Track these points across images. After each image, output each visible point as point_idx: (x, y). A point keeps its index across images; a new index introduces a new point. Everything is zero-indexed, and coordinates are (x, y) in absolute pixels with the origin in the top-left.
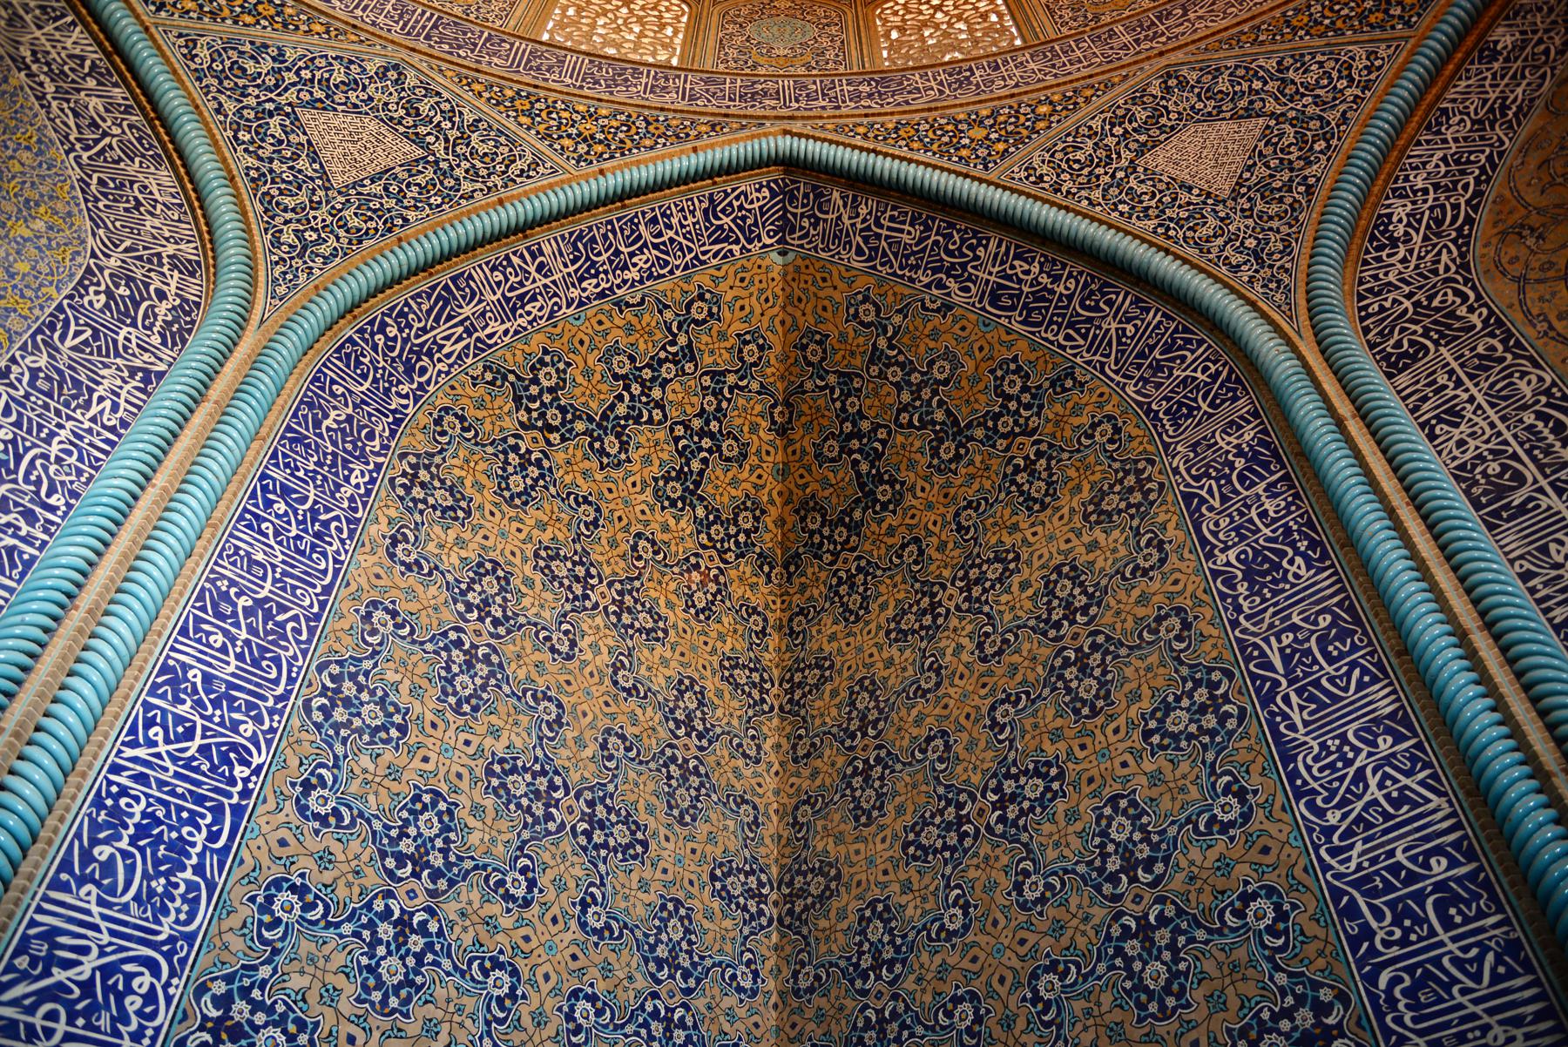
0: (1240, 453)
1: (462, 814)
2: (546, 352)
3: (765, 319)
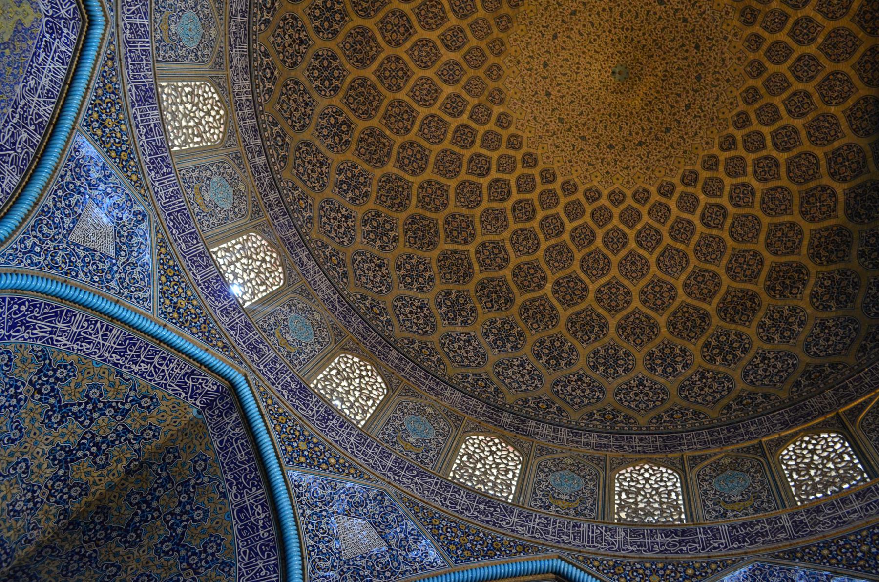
2: (71, 364)
3: (168, 428)
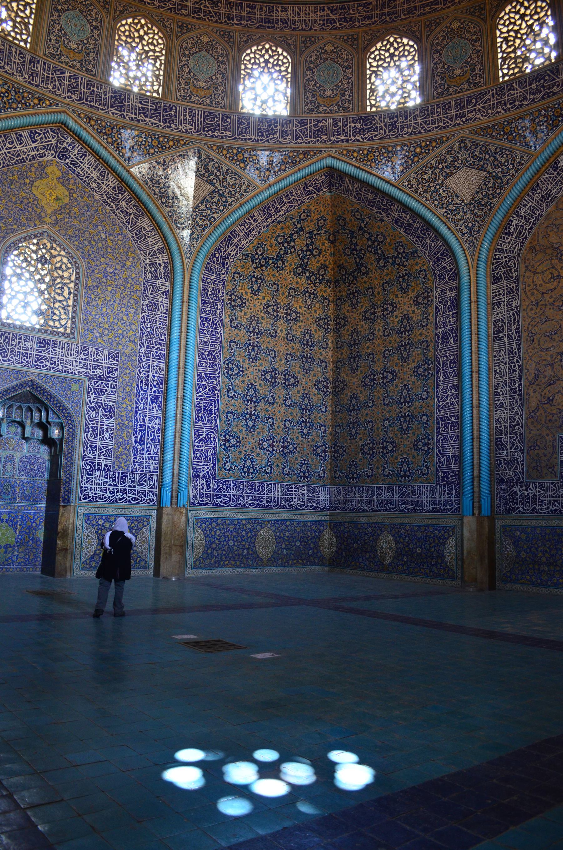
0: (450, 300)
1: (258, 387)
